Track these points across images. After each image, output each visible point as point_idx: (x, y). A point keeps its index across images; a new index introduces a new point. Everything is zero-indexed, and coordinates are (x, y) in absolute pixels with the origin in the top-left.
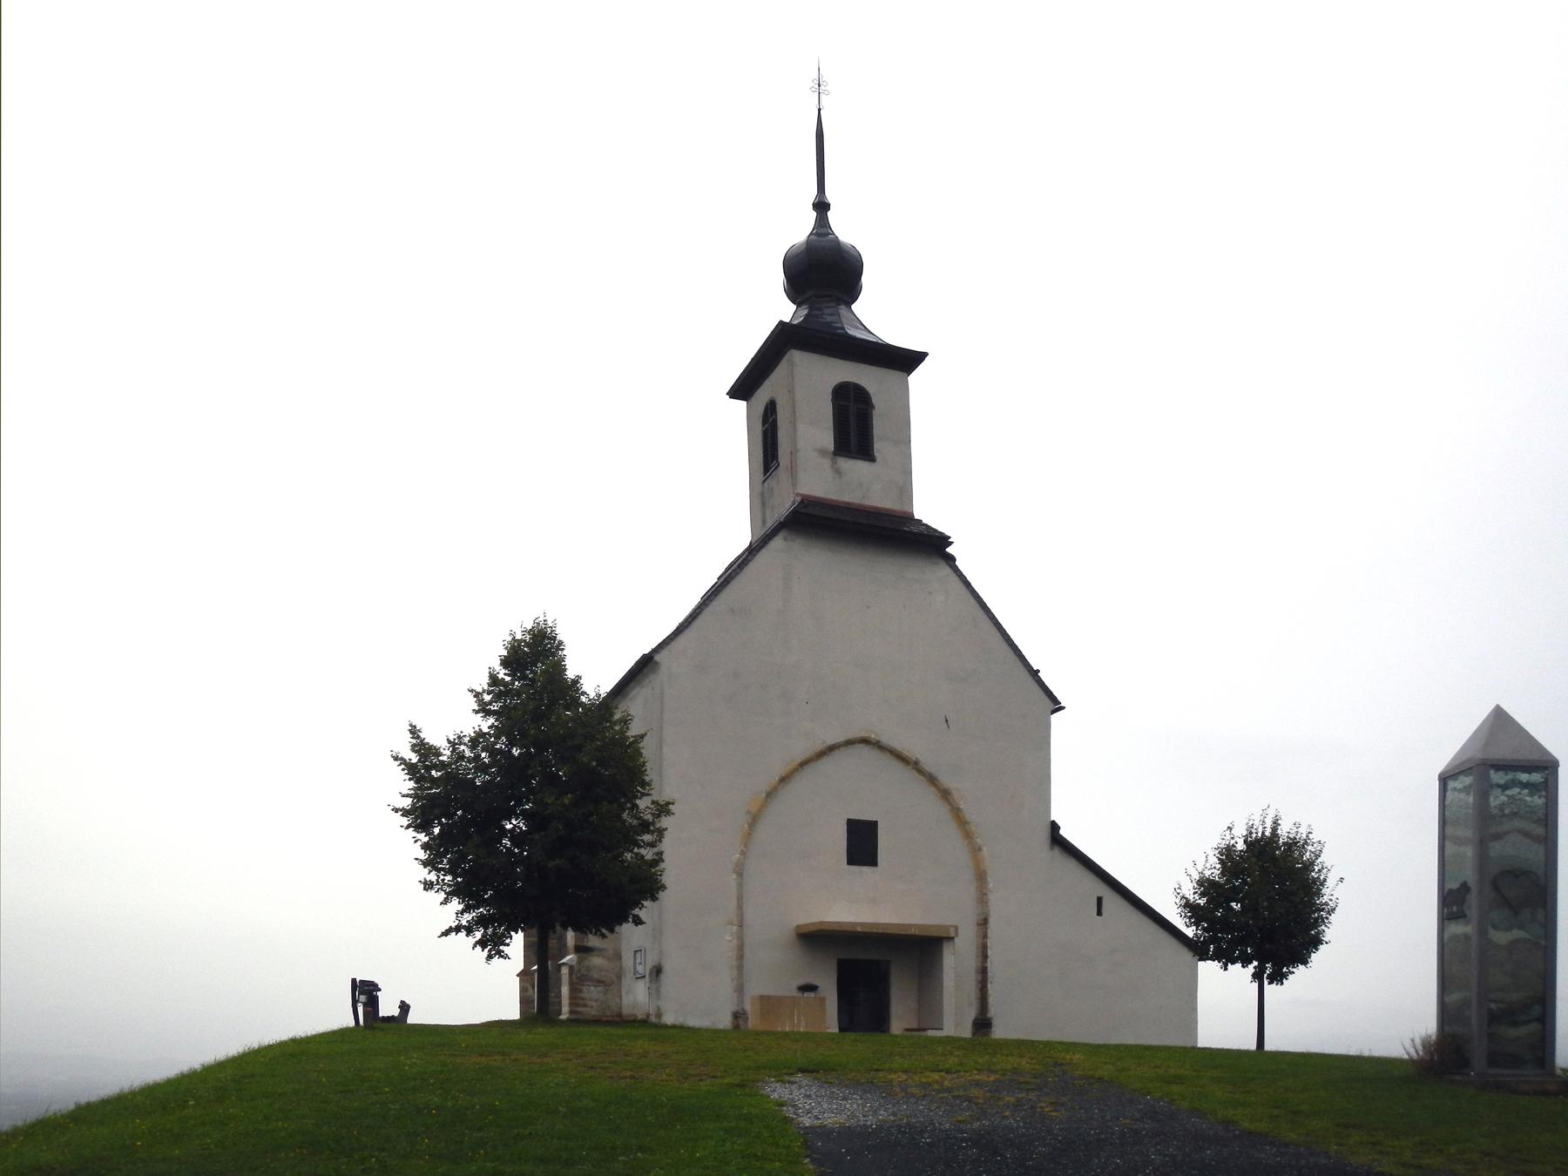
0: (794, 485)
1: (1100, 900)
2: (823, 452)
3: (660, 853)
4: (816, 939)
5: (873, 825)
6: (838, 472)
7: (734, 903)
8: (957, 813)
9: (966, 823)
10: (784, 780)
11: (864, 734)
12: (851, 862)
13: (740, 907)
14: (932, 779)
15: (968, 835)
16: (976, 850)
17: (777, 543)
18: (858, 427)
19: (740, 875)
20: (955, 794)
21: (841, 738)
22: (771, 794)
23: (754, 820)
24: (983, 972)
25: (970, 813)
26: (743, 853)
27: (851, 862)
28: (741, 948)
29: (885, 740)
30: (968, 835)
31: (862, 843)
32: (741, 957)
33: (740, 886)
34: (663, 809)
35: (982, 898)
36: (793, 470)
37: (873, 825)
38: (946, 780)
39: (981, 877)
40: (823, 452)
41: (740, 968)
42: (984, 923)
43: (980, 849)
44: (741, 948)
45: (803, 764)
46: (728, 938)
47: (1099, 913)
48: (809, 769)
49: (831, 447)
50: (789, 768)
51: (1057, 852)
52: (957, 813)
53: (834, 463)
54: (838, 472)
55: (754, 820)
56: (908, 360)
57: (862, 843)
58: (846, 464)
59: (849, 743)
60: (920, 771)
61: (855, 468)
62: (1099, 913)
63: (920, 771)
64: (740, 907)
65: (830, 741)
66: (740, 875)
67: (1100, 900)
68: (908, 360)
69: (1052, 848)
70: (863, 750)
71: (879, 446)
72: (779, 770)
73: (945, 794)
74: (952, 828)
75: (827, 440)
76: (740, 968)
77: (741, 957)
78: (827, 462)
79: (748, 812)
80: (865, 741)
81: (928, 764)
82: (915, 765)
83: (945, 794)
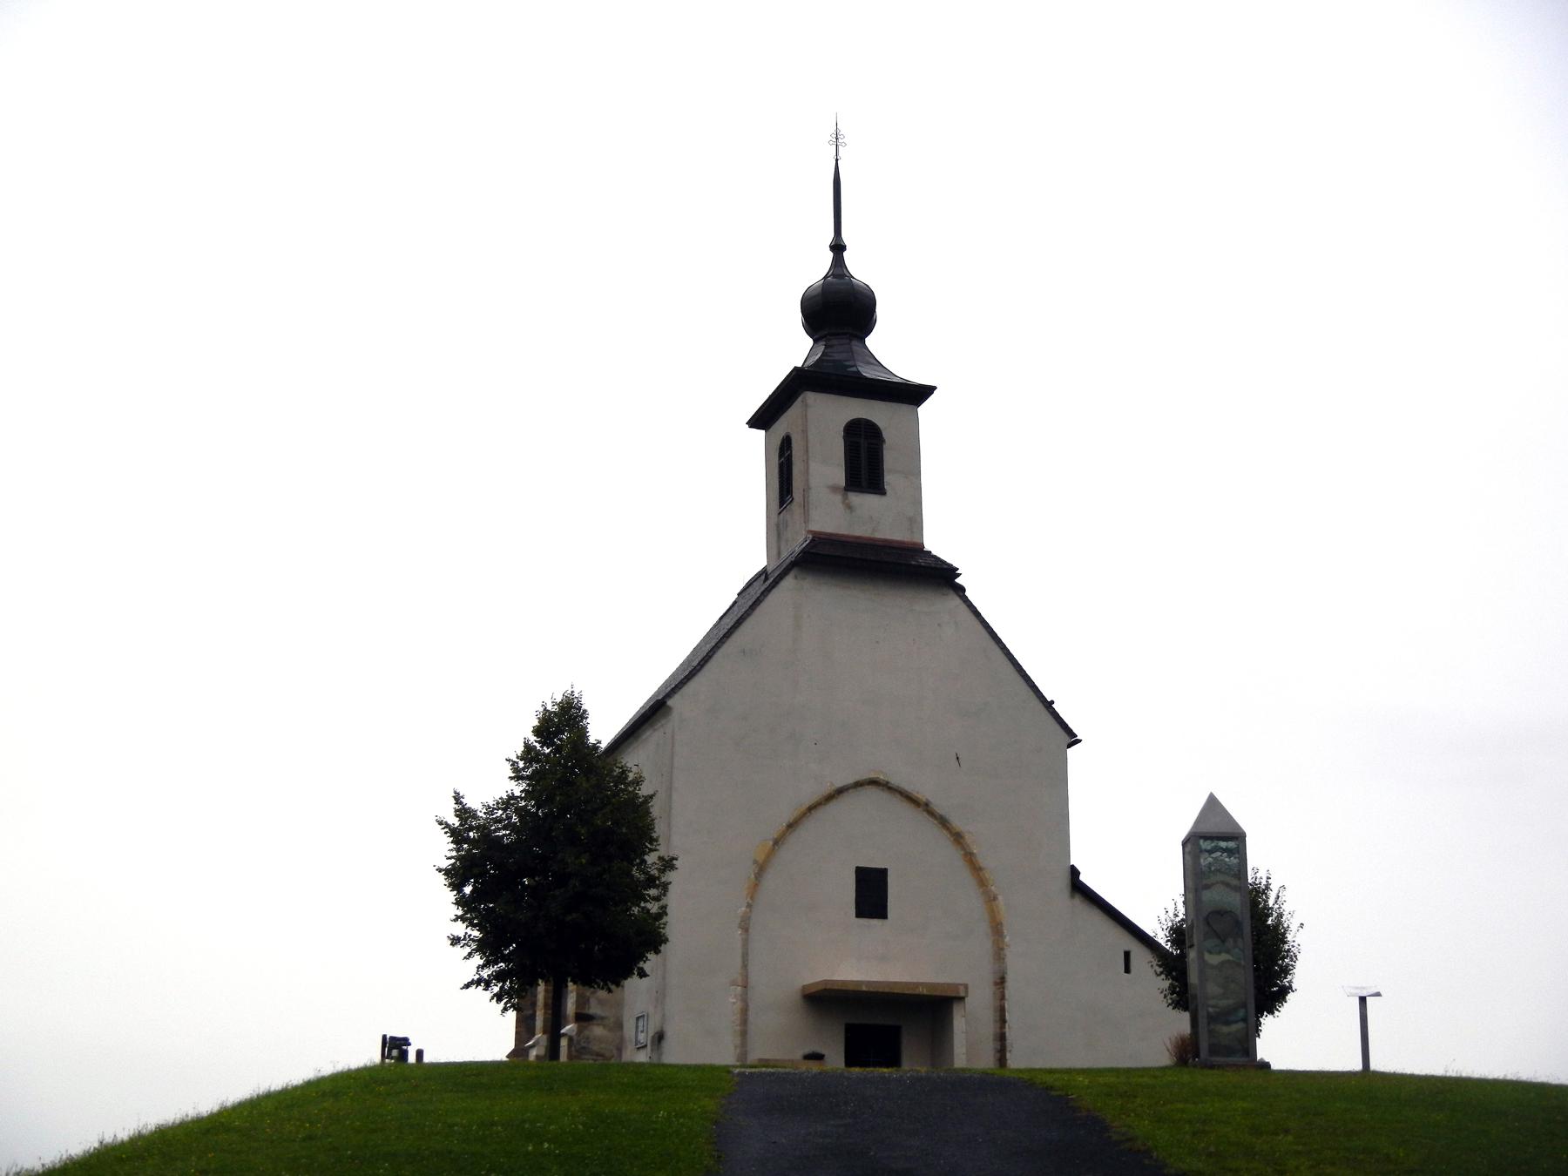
0: (806, 521)
1: (1127, 955)
2: (834, 489)
3: (664, 908)
4: (825, 1001)
5: (882, 874)
6: (849, 507)
7: (739, 960)
8: (969, 857)
9: (980, 869)
10: (791, 826)
11: (873, 775)
12: (858, 916)
13: (745, 966)
14: (943, 822)
15: (982, 883)
16: (991, 899)
17: (789, 582)
18: (870, 462)
19: (746, 930)
20: (968, 839)
21: (851, 780)
22: (777, 842)
23: (761, 869)
24: (1002, 1038)
25: (985, 859)
26: (749, 906)
27: (858, 916)
28: (745, 1011)
29: (895, 781)
30: (982, 883)
31: (871, 894)
32: (744, 1021)
33: (746, 943)
34: (668, 864)
35: (999, 954)
36: (805, 506)
37: (882, 874)
38: (957, 823)
39: (997, 930)
40: (834, 489)
41: (744, 1034)
42: (1001, 982)
43: (995, 898)
44: (745, 1011)
45: (811, 809)
46: (732, 1001)
47: (1127, 970)
48: (820, 814)
49: (843, 483)
50: (796, 814)
51: (1078, 901)
52: (969, 857)
53: (845, 498)
54: (849, 507)
55: (761, 869)
56: (917, 394)
57: (871, 894)
58: (856, 499)
59: (858, 785)
60: (931, 813)
61: (865, 502)
62: (1127, 970)
63: (931, 813)
64: (745, 966)
65: (839, 784)
66: (746, 930)
67: (1127, 955)
68: (917, 394)
69: (1072, 896)
70: (872, 792)
71: (889, 479)
72: (787, 816)
73: (958, 838)
74: (966, 874)
75: (840, 477)
76: (744, 1034)
77: (744, 1021)
78: (838, 498)
79: (755, 862)
80: (874, 782)
81: (940, 806)
82: (925, 807)
83: (958, 838)
